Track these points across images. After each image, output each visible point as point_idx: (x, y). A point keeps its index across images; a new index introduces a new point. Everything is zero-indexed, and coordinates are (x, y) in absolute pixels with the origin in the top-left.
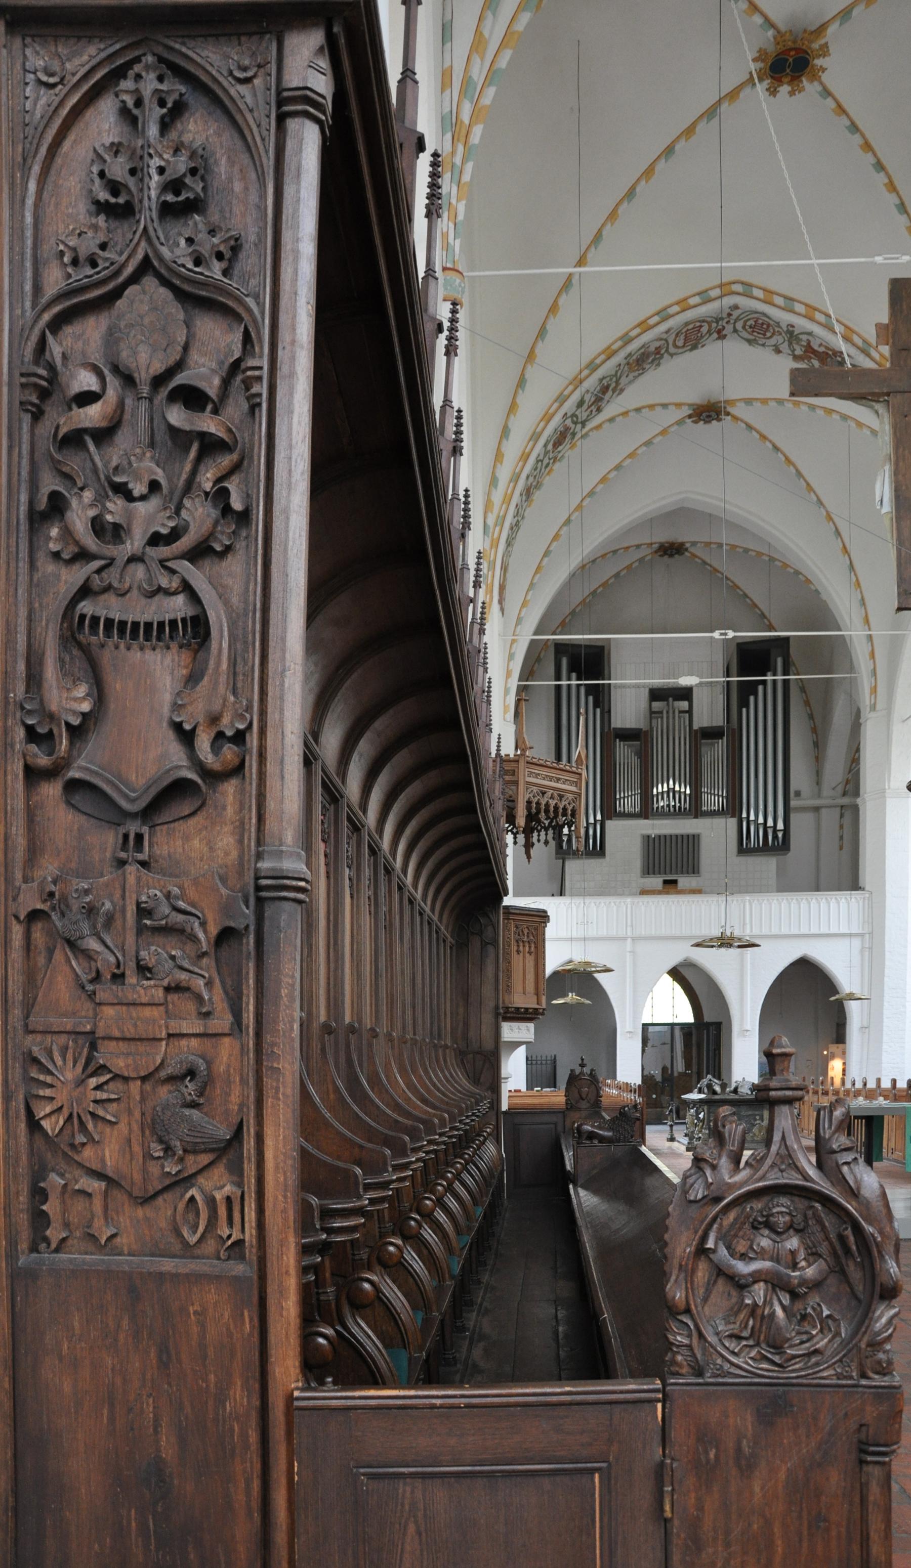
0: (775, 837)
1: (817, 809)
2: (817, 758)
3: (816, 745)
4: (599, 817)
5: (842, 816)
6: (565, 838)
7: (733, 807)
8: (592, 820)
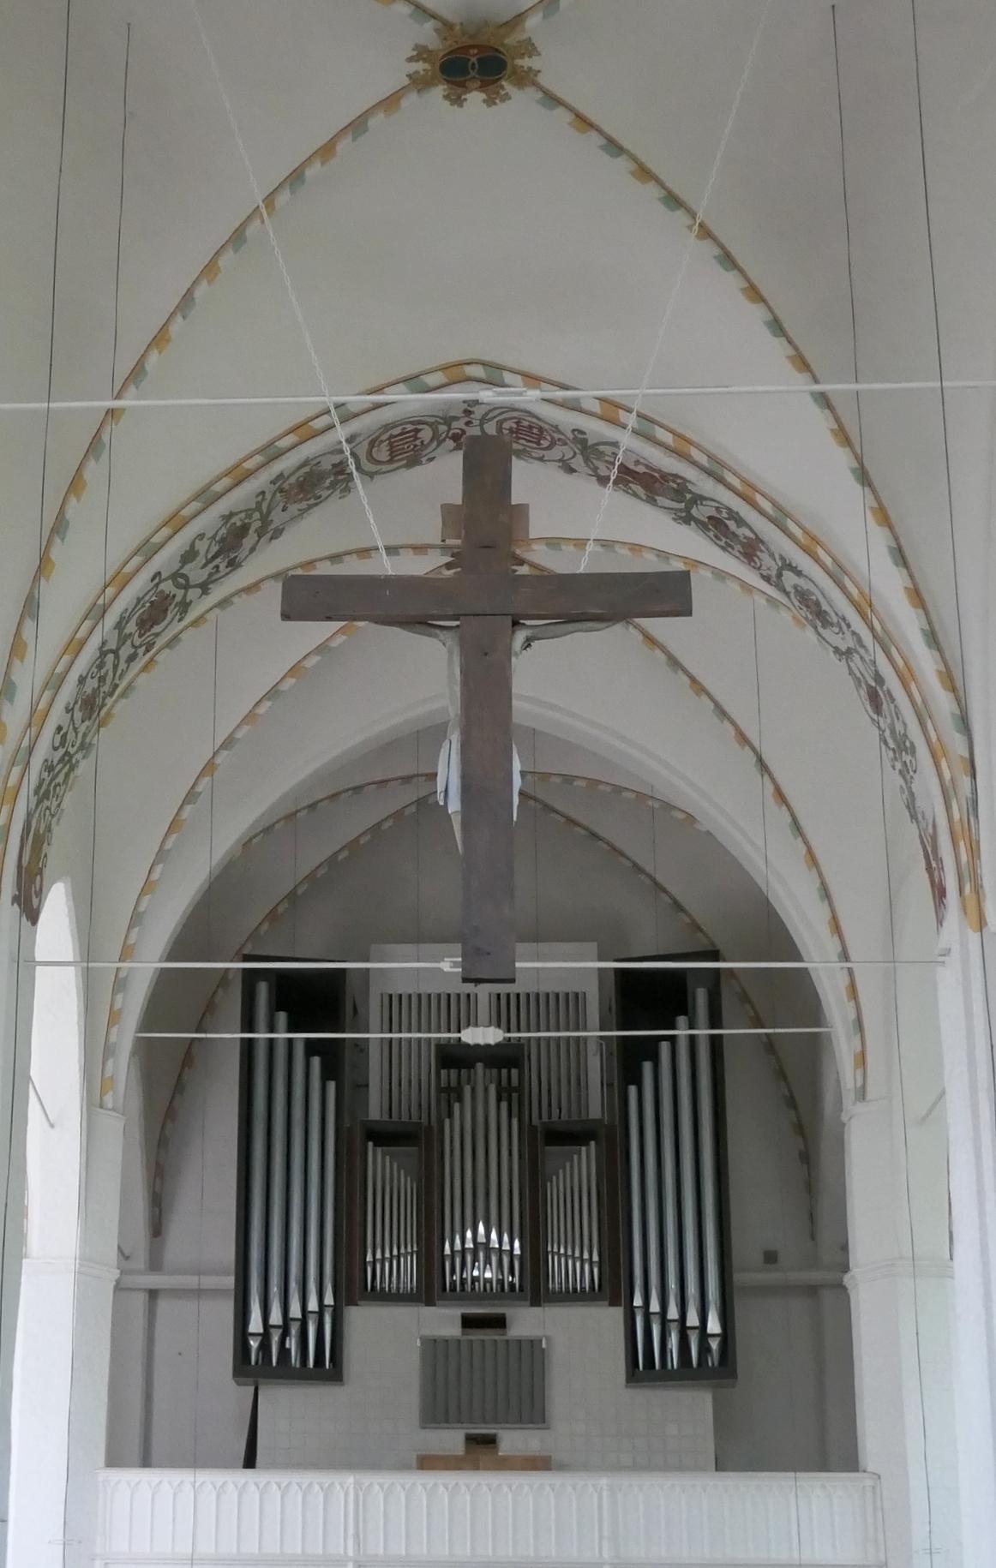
0: (704, 1349)
4: (329, 1299)
6: (254, 1344)
8: (313, 1305)
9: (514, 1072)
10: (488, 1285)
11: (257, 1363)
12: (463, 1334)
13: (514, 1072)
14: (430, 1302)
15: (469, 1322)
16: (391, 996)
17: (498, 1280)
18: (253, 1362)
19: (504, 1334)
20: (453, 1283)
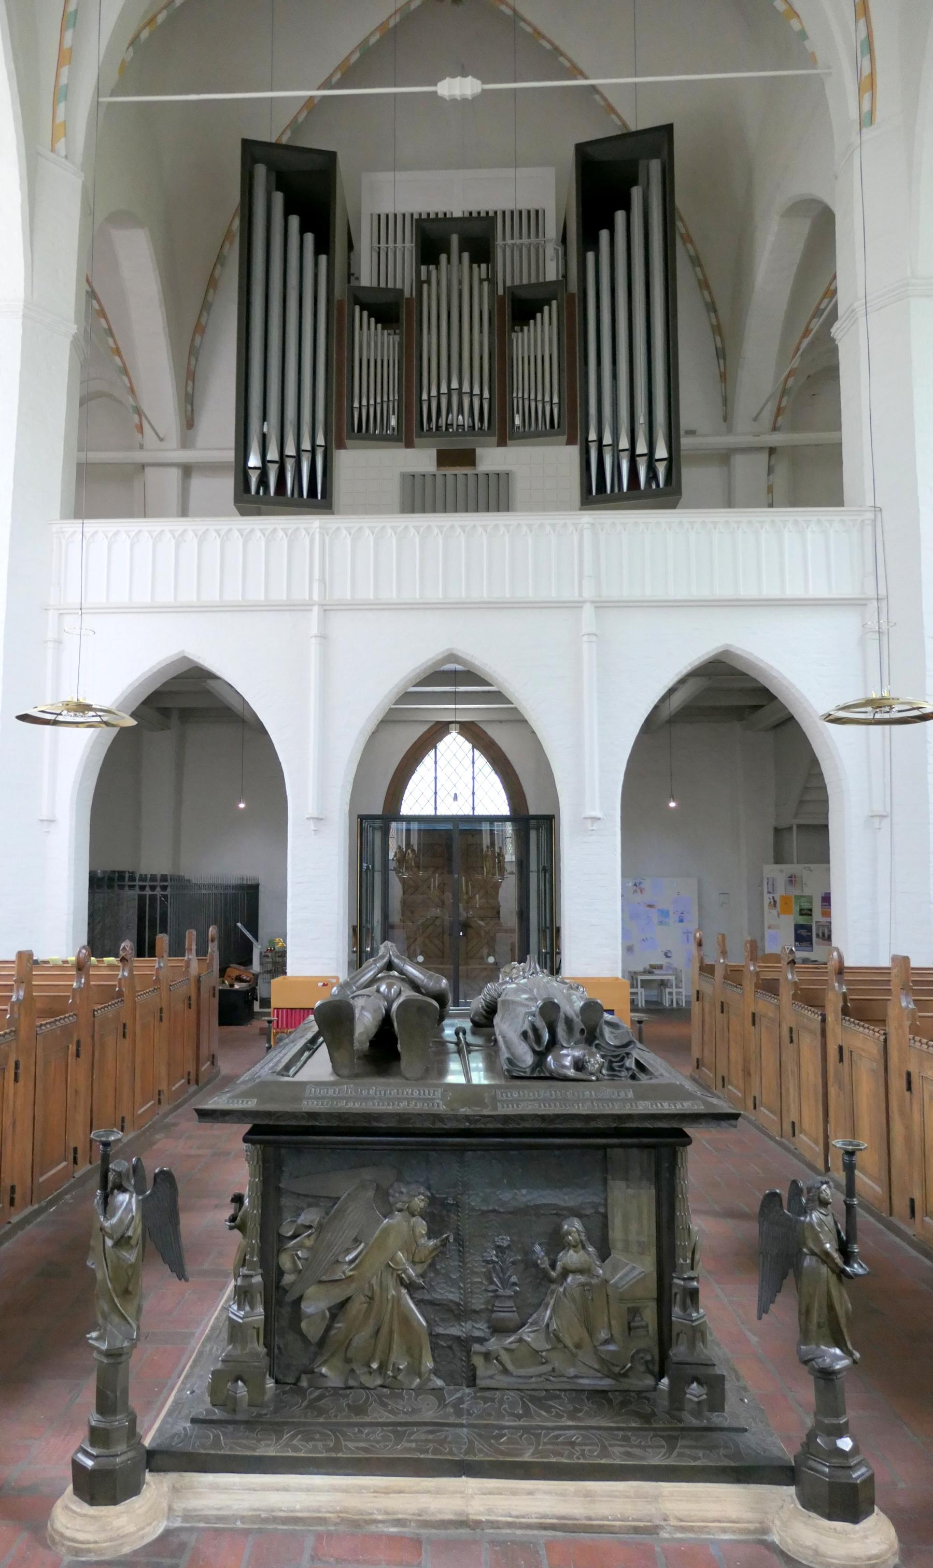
1: (725, 457)
2: (723, 377)
3: (721, 353)
4: (320, 440)
5: (770, 470)
8: (306, 445)
11: (258, 492)
12: (438, 470)
13: (483, 266)
14: (409, 444)
15: (445, 458)
17: (469, 427)
19: (475, 469)
20: (430, 429)
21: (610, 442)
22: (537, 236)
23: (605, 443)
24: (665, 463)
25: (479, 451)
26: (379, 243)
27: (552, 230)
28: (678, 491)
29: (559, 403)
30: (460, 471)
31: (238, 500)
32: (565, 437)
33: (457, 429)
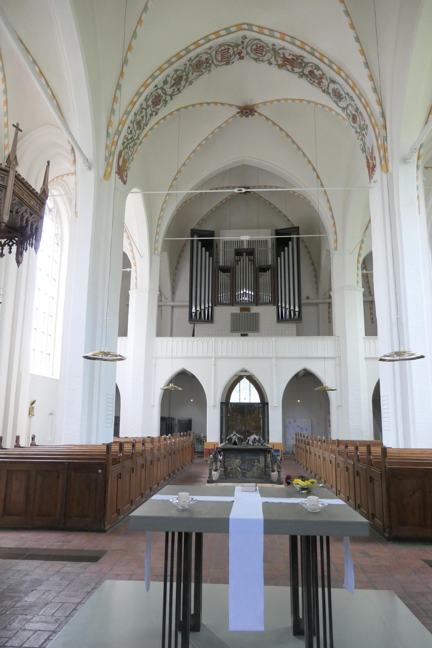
0: (295, 314)
4: (210, 305)
6: (193, 314)
7: (274, 301)
8: (207, 306)
9: (252, 257)
10: (246, 302)
11: (194, 318)
13: (252, 257)
14: (233, 305)
15: (242, 310)
16: (225, 241)
17: (248, 301)
18: (193, 318)
19: (250, 312)
20: (238, 301)
21: (284, 306)
22: (266, 247)
23: (283, 306)
24: (298, 312)
25: (251, 307)
26: (225, 249)
27: (270, 246)
28: (301, 320)
29: (271, 296)
30: (246, 313)
31: (189, 321)
32: (273, 305)
33: (245, 302)
